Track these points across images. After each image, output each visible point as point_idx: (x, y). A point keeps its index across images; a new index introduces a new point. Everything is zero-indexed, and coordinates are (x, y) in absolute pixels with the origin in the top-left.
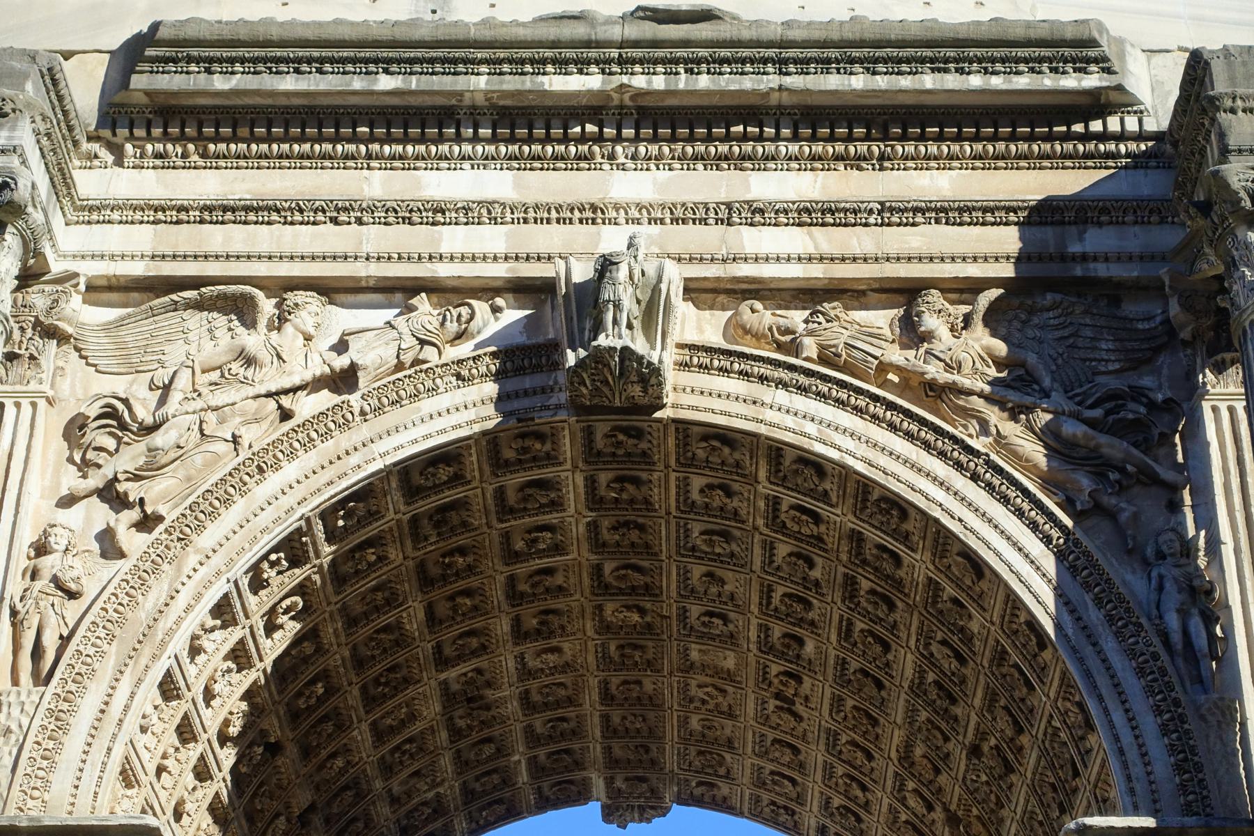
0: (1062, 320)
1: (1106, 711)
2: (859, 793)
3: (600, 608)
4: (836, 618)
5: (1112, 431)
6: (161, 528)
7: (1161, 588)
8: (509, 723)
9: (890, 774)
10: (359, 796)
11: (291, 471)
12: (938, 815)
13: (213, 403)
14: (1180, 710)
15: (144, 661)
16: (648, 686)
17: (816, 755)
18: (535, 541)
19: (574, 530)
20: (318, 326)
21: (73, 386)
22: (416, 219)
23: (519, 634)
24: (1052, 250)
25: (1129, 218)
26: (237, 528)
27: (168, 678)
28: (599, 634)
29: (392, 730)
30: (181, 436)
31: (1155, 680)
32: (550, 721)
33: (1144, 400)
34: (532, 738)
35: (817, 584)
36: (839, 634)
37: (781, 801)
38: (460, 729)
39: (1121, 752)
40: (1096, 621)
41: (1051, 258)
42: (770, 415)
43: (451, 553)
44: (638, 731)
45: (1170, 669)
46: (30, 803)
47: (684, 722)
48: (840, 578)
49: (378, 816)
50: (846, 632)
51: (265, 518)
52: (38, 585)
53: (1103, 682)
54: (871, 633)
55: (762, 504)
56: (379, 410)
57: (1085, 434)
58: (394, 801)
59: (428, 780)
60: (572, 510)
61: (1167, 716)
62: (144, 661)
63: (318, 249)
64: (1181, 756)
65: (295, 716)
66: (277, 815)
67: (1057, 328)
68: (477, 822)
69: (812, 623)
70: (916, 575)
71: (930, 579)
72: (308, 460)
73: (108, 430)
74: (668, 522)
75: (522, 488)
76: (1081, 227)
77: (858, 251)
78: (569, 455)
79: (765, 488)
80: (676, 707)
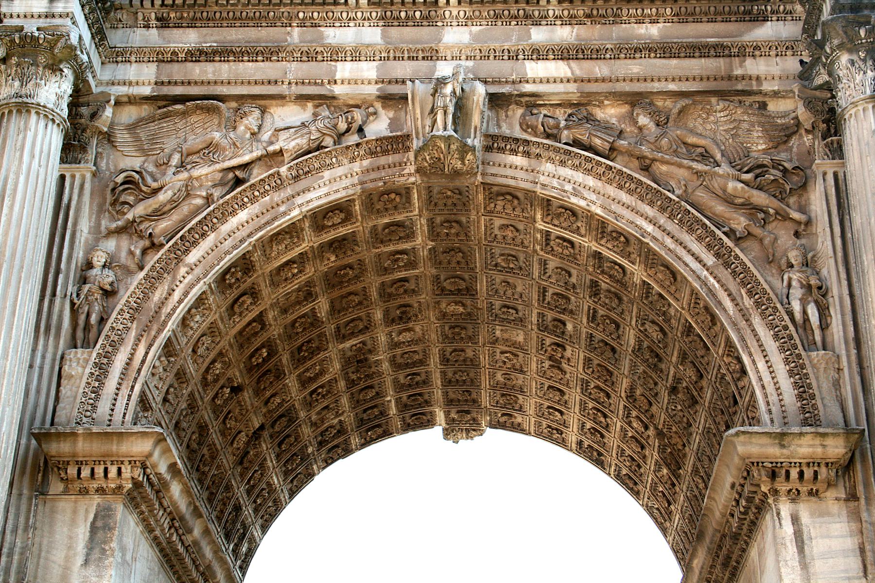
1: (754, 361)
2: (602, 419)
3: (438, 303)
4: (586, 308)
5: (760, 188)
6: (162, 251)
7: (789, 286)
8: (383, 376)
9: (621, 407)
10: (291, 421)
11: (243, 215)
12: (651, 432)
14: (801, 361)
15: (153, 333)
16: (470, 353)
17: (574, 396)
18: (397, 260)
19: (421, 254)
21: (108, 164)
22: (320, 58)
23: (389, 320)
24: (723, 74)
25: (773, 53)
26: (210, 252)
27: (169, 343)
28: (439, 320)
29: (311, 380)
30: (175, 194)
32: (409, 375)
33: (781, 168)
34: (399, 387)
35: (574, 287)
36: (588, 319)
37: (554, 425)
38: (353, 380)
39: (763, 387)
40: (748, 306)
42: (542, 179)
43: (345, 267)
44: (464, 381)
45: (795, 335)
46: (85, 420)
47: (492, 376)
48: (588, 282)
49: (303, 434)
50: (593, 317)
51: (228, 244)
52: (86, 287)
54: (608, 317)
55: (539, 236)
56: (296, 178)
57: (742, 188)
58: (314, 425)
59: (334, 412)
60: (419, 240)
61: (793, 365)
63: (258, 77)
64: (801, 389)
65: (250, 369)
66: (240, 432)
68: (365, 439)
69: (571, 312)
70: (635, 279)
71: (644, 282)
73: (129, 191)
74: (480, 248)
75: (388, 226)
76: (742, 58)
78: (417, 205)
79: (540, 225)
80: (487, 366)
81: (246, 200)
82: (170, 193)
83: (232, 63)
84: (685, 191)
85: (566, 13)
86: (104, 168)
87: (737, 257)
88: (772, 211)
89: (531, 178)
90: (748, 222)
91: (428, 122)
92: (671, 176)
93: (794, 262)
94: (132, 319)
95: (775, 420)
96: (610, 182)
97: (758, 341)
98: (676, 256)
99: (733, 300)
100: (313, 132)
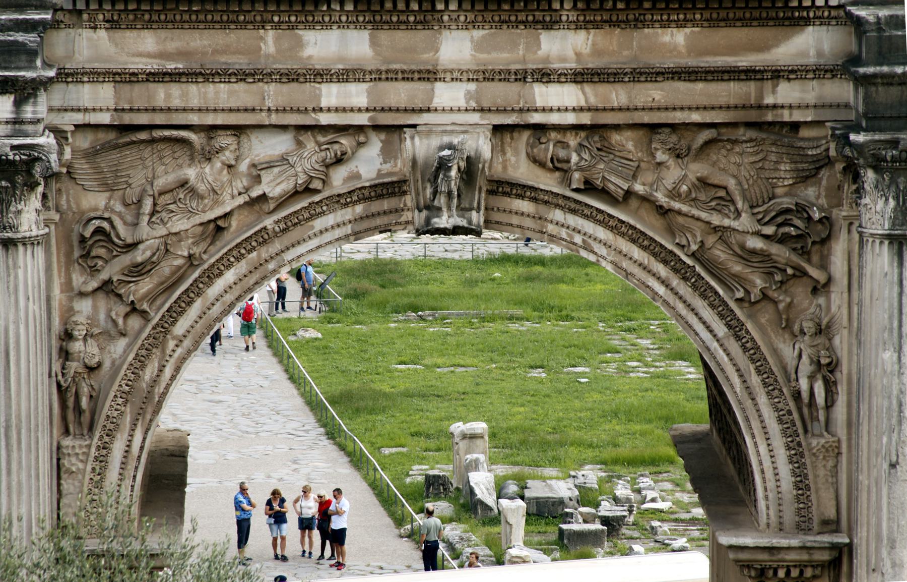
0: (756, 148)
11: (230, 276)
13: (174, 230)
14: (801, 450)
15: (148, 417)
20: (237, 159)
21: (68, 201)
22: (301, 79)
25: (811, 75)
26: (198, 320)
30: (154, 254)
31: (788, 428)
33: (805, 215)
39: (763, 472)
41: (751, 107)
53: (755, 424)
56: (284, 231)
61: (793, 452)
62: (148, 417)
64: (799, 479)
67: (752, 154)
72: (241, 267)
76: (775, 81)
77: (616, 104)
81: (232, 259)
82: (148, 254)
83: (200, 85)
84: (700, 247)
85: (581, 18)
86: (65, 207)
87: (747, 332)
88: (790, 271)
89: (538, 228)
90: (764, 285)
91: (429, 191)
92: (689, 229)
93: (806, 330)
94: (125, 404)
95: (771, 508)
96: (622, 235)
97: (762, 422)
98: (687, 323)
99: (741, 376)
100: (300, 174)
